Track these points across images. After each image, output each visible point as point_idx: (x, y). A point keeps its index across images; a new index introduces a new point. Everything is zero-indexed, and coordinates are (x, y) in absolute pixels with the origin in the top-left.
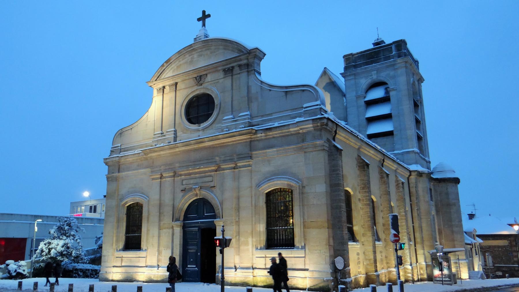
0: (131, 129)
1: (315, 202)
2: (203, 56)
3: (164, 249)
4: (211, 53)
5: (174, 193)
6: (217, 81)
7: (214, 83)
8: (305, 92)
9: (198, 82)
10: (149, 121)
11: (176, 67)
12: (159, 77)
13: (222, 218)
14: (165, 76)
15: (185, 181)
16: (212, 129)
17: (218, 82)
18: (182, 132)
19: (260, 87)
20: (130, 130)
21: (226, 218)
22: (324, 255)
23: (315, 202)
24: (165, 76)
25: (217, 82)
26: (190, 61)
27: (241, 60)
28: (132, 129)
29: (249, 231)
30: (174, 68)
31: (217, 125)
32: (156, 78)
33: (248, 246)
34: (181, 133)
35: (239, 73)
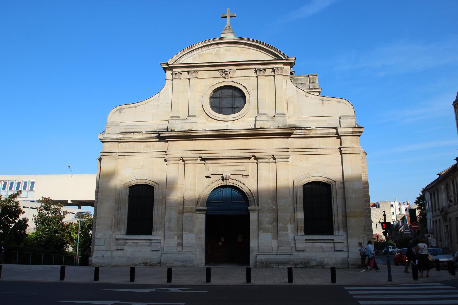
0: (136, 107)
1: (353, 196)
2: (231, 51)
4: (241, 50)
7: (245, 79)
8: (341, 104)
10: (161, 103)
11: (197, 55)
12: (177, 61)
13: (258, 205)
14: (183, 61)
17: (250, 79)
18: (205, 119)
19: (296, 92)
21: (262, 206)
22: (363, 239)
23: (353, 196)
24: (183, 61)
25: (248, 79)
26: (215, 53)
28: (137, 107)
29: (288, 219)
30: (195, 56)
31: (248, 119)
32: (174, 61)
33: (287, 231)
34: (205, 120)
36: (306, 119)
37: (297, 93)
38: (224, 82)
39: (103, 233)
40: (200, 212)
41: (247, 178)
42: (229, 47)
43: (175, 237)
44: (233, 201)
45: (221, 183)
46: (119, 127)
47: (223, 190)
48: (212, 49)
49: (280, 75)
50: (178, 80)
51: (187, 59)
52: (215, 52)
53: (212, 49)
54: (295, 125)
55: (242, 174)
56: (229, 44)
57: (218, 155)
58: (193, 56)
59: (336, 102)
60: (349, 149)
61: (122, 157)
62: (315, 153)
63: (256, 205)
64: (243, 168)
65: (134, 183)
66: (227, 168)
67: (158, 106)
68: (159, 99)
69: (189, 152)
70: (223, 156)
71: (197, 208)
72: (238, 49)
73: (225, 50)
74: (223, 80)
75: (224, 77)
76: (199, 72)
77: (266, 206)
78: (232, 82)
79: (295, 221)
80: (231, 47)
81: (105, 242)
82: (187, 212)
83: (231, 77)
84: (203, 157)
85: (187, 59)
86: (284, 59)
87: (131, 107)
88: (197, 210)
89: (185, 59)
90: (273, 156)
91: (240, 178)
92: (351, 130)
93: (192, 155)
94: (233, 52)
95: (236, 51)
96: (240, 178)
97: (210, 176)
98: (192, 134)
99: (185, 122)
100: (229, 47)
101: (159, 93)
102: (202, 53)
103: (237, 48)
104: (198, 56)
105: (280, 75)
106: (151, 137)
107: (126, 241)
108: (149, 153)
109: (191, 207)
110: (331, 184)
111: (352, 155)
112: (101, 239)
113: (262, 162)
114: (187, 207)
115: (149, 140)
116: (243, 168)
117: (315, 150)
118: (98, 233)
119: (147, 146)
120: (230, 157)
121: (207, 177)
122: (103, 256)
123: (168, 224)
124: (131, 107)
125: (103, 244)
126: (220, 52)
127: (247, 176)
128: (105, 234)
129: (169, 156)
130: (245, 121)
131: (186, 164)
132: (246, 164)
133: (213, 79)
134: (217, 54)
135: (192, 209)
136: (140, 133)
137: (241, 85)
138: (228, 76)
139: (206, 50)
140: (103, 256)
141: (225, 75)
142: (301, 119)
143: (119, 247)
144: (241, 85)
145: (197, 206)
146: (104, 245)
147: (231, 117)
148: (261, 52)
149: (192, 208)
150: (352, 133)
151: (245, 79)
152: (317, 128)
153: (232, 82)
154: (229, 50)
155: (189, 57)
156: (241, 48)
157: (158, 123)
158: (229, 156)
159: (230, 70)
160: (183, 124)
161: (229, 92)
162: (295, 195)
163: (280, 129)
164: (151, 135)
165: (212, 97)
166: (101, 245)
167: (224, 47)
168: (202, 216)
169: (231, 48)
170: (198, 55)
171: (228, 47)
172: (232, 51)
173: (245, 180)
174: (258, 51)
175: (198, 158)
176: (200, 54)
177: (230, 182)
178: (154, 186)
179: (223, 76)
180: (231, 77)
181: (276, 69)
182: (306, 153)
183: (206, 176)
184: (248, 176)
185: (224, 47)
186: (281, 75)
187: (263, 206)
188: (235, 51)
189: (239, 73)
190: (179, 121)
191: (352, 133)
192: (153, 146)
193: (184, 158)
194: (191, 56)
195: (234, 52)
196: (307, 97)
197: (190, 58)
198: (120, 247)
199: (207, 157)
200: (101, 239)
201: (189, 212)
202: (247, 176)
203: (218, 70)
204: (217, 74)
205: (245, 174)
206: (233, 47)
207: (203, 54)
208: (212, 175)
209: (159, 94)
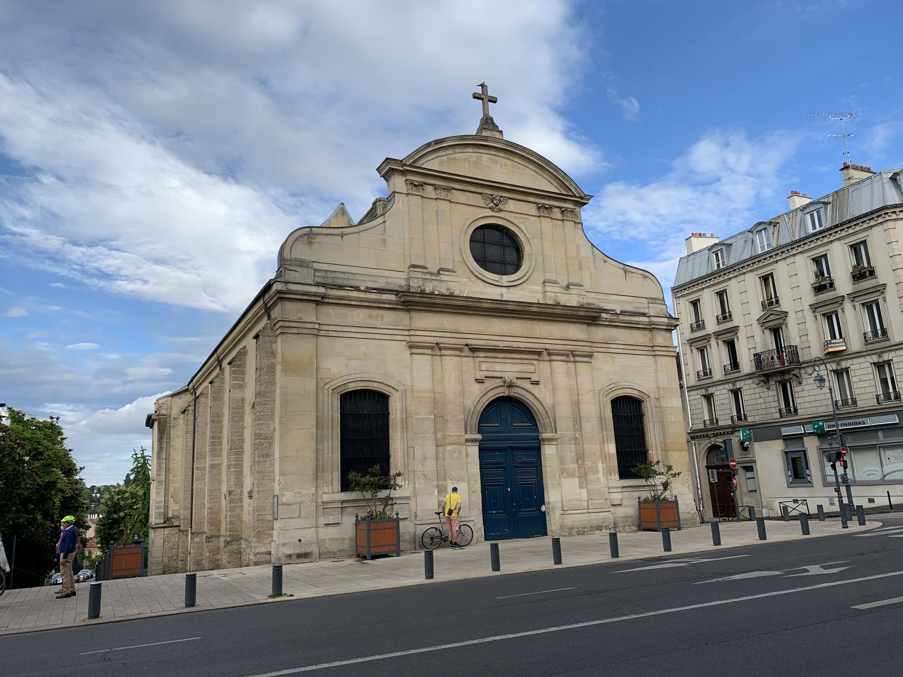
3: (451, 482)
4: (513, 166)
5: (461, 381)
6: (525, 216)
7: (521, 218)
9: (497, 206)
13: (556, 432)
14: (423, 164)
15: (484, 364)
16: (524, 290)
17: (528, 219)
18: (466, 278)
20: (338, 237)
24: (423, 164)
27: (565, 200)
30: (441, 158)
31: (530, 287)
34: (466, 280)
35: (563, 220)
36: (606, 297)
37: (593, 254)
38: (492, 216)
39: (295, 492)
40: (472, 444)
41: (536, 385)
42: (495, 155)
43: (435, 491)
44: (514, 425)
45: (503, 392)
46: (313, 272)
47: (497, 405)
48: (469, 152)
49: (571, 221)
50: (417, 197)
51: (429, 161)
52: (475, 159)
53: (469, 152)
54: (594, 304)
55: (530, 378)
56: (495, 151)
57: (498, 343)
58: (439, 158)
59: (640, 276)
60: (663, 349)
61: (295, 331)
62: (621, 351)
63: (554, 432)
64: (531, 368)
65: (352, 387)
66: (508, 367)
67: (384, 241)
68: (385, 228)
69: (449, 335)
70: (504, 347)
71: (469, 436)
72: (509, 163)
73: (490, 159)
74: (490, 213)
75: (490, 208)
76: (453, 190)
77: (568, 433)
78: (504, 219)
79: (605, 457)
80: (498, 156)
81: (302, 510)
82: (451, 444)
83: (502, 210)
84: (471, 345)
85: (429, 161)
86: (578, 195)
87: (333, 235)
88: (467, 441)
89: (427, 162)
90: (572, 352)
91: (526, 384)
92: (666, 320)
93: (453, 341)
94: (502, 166)
95: (506, 165)
96: (526, 384)
97: (483, 380)
98: (458, 303)
99: (439, 278)
100: (495, 155)
101: (383, 216)
102: (453, 156)
103: (507, 160)
104: (448, 161)
105: (571, 221)
106: (382, 300)
107: (344, 506)
108: (376, 331)
109: (458, 434)
110: (644, 400)
111: (667, 358)
112: (292, 504)
113: (557, 361)
114: (452, 434)
115: (377, 305)
116: (531, 368)
117: (621, 347)
118: (285, 493)
119: (370, 317)
120: (514, 347)
121: (478, 381)
122: (300, 540)
123: (421, 466)
124: (333, 235)
125: (298, 516)
126: (483, 161)
127: (536, 383)
128: (300, 492)
129: (414, 339)
130: (526, 290)
131: (445, 355)
132: (535, 362)
133: (475, 208)
134: (477, 164)
135: (459, 437)
136: (357, 289)
137: (518, 227)
138: (497, 207)
139: (459, 153)
140: (300, 540)
141: (491, 205)
142: (600, 296)
143: (330, 518)
144: (518, 227)
145: (466, 433)
146: (300, 517)
147: (506, 280)
148: (543, 177)
149: (459, 436)
150: (667, 326)
151: (521, 218)
152: (623, 313)
153: (504, 219)
154: (496, 162)
155: (433, 159)
156: (513, 162)
157: (387, 273)
158: (512, 347)
159: (501, 197)
160: (435, 283)
161: (495, 235)
162: (602, 415)
163: (584, 310)
164: (380, 296)
165: (472, 240)
166: (293, 518)
167: (488, 154)
168: (474, 450)
169: (499, 158)
170: (448, 158)
171: (493, 155)
172: (501, 164)
173: (535, 390)
174: (538, 173)
175: (463, 346)
176: (450, 158)
177: (514, 392)
178: (389, 394)
179: (490, 206)
180: (502, 210)
181: (566, 209)
182: (612, 351)
183: (477, 380)
184: (538, 382)
185: (488, 154)
186: (573, 221)
187: (564, 433)
188: (504, 166)
189: (511, 205)
190: (428, 276)
191: (667, 326)
192: (382, 317)
193: (443, 344)
194: (436, 158)
195: (503, 167)
196: (607, 263)
197: (435, 160)
198: (332, 519)
199: (480, 345)
200: (292, 504)
201: (455, 444)
202: (536, 383)
203: (481, 194)
204: (478, 200)
205: (534, 378)
206: (502, 159)
207: (455, 158)
208: (486, 377)
209: (384, 218)
